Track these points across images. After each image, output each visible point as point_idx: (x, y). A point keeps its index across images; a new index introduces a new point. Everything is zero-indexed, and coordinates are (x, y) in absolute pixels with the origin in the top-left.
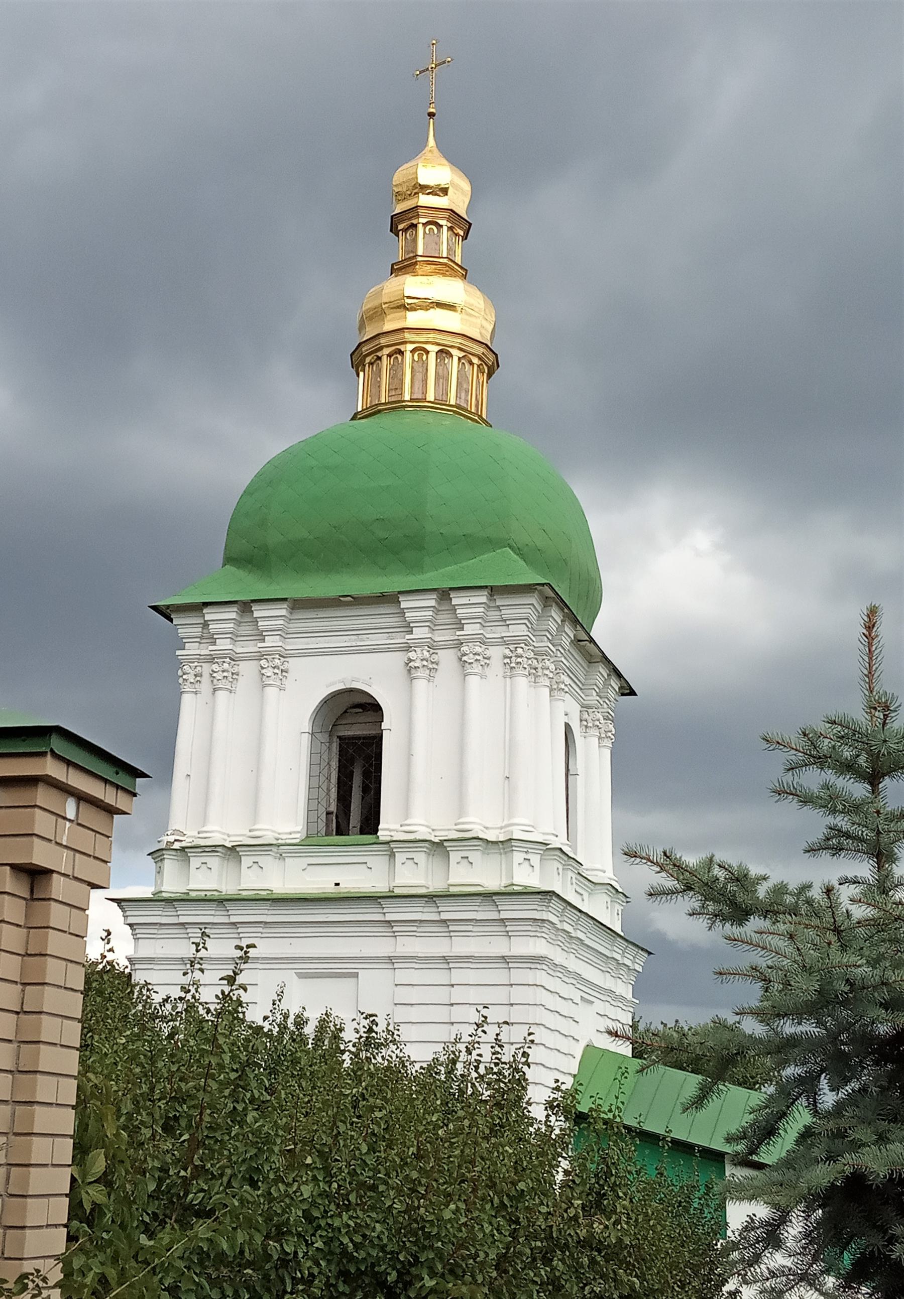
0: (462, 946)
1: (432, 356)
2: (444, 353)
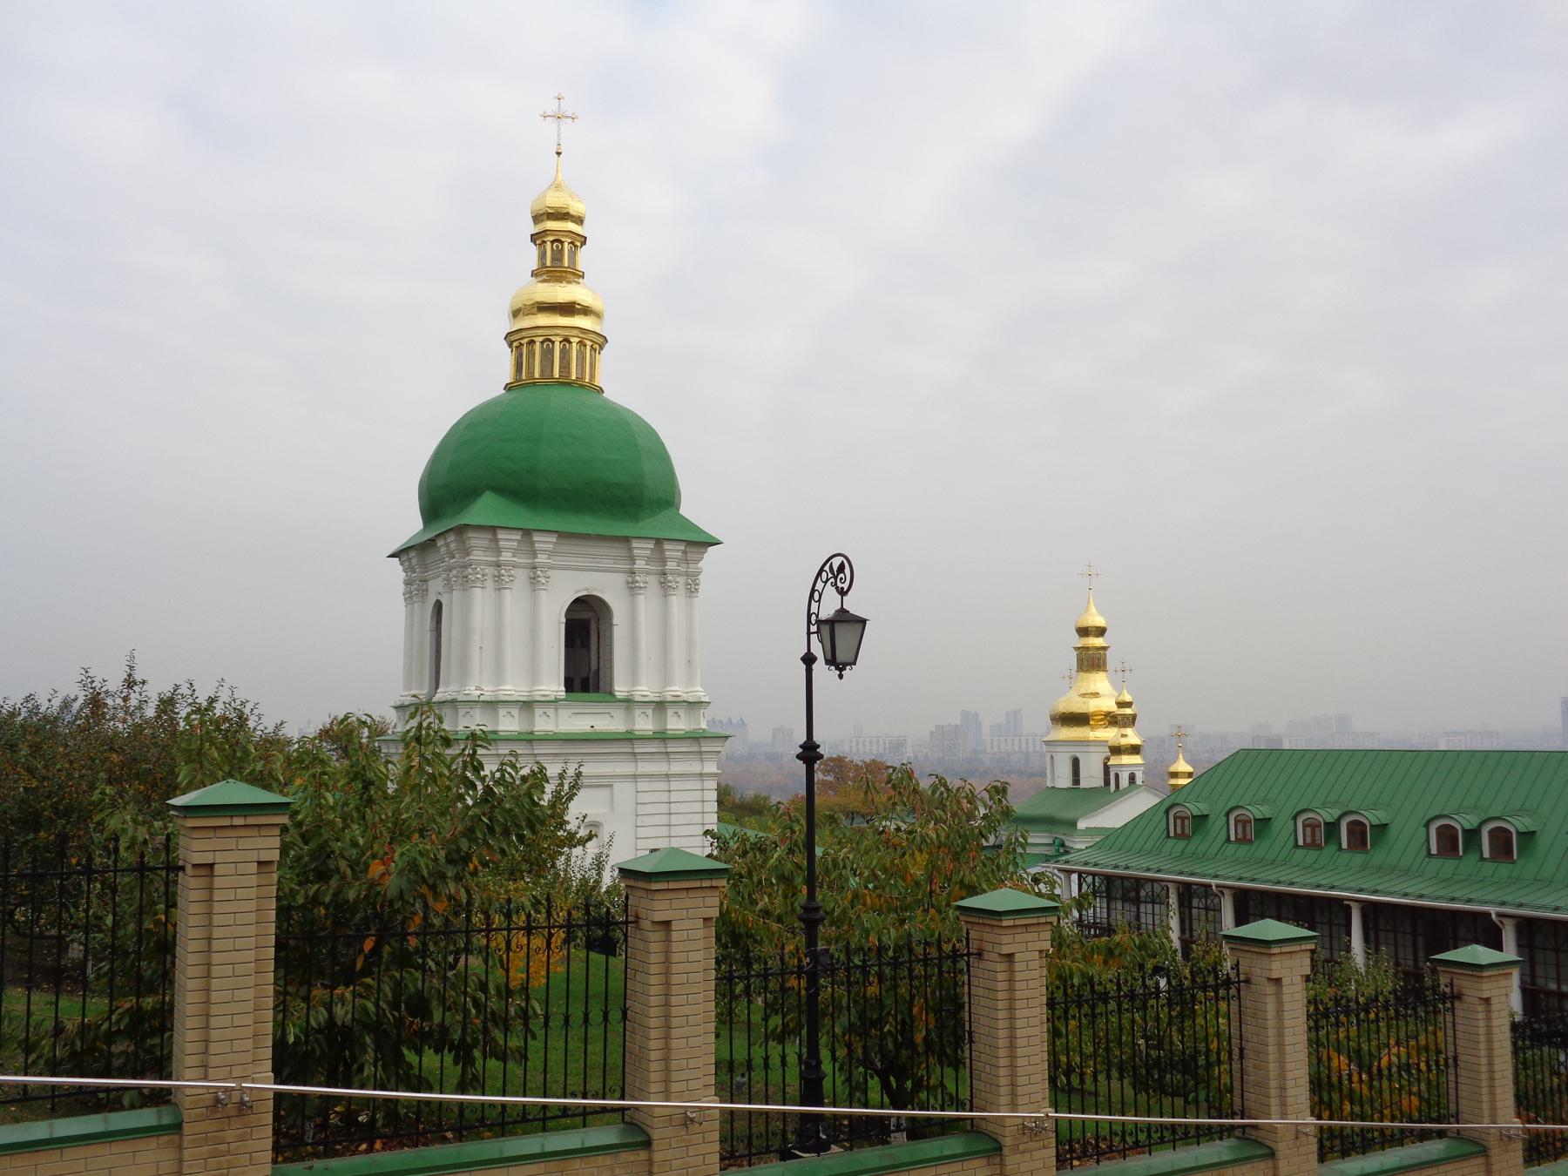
0: (677, 767)
2: (582, 343)
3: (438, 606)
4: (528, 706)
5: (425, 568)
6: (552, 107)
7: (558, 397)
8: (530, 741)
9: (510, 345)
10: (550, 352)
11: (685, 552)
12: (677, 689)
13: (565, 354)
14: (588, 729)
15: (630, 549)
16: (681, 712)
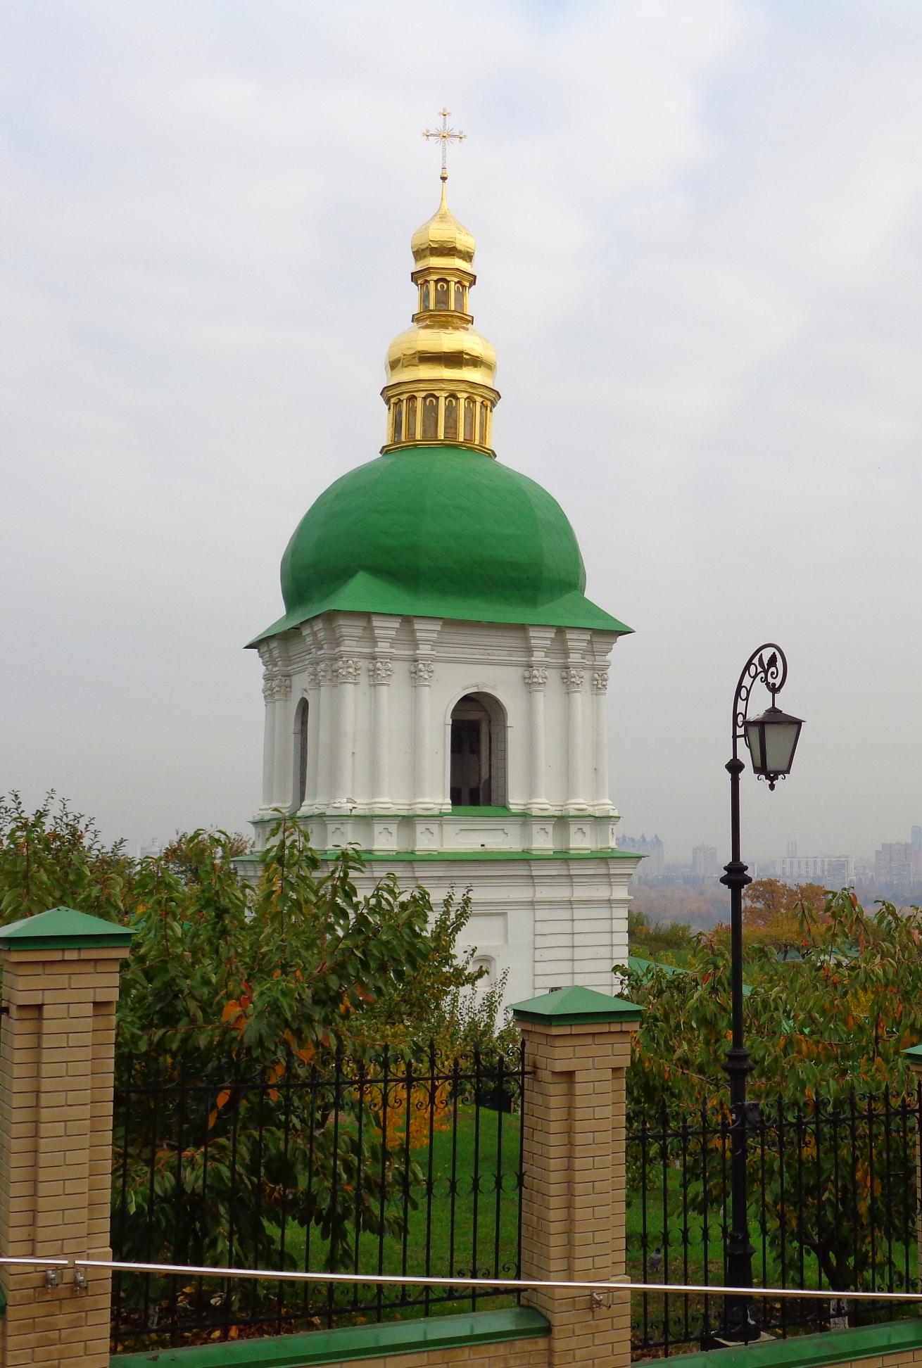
0: (581, 893)
1: (478, 405)
2: (470, 399)
3: (304, 706)
4: (407, 821)
5: (288, 661)
6: (436, 124)
7: (445, 463)
8: (410, 862)
9: (388, 402)
10: (433, 410)
11: (590, 642)
12: (582, 802)
13: (451, 412)
14: (478, 848)
15: (527, 639)
16: (586, 828)
